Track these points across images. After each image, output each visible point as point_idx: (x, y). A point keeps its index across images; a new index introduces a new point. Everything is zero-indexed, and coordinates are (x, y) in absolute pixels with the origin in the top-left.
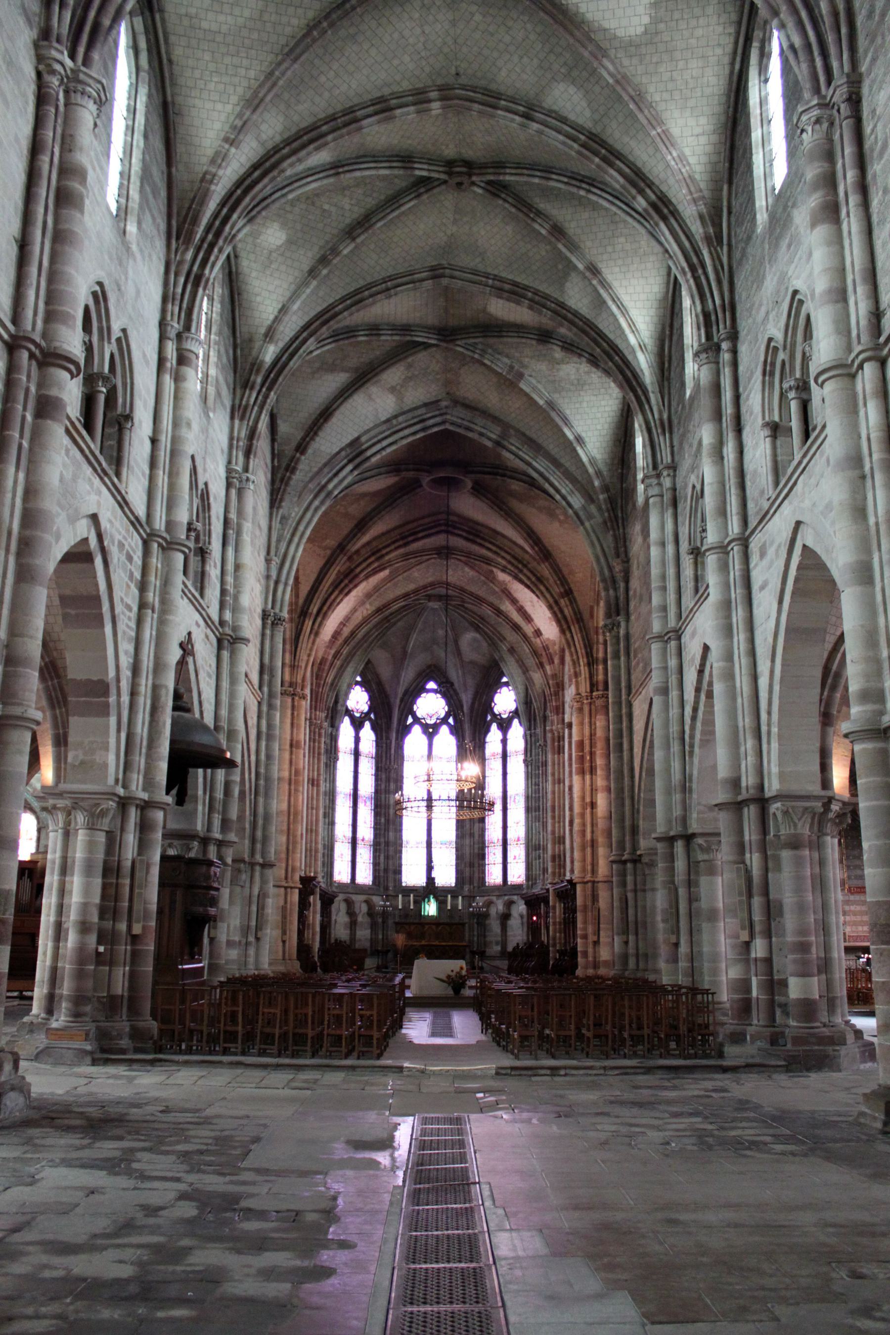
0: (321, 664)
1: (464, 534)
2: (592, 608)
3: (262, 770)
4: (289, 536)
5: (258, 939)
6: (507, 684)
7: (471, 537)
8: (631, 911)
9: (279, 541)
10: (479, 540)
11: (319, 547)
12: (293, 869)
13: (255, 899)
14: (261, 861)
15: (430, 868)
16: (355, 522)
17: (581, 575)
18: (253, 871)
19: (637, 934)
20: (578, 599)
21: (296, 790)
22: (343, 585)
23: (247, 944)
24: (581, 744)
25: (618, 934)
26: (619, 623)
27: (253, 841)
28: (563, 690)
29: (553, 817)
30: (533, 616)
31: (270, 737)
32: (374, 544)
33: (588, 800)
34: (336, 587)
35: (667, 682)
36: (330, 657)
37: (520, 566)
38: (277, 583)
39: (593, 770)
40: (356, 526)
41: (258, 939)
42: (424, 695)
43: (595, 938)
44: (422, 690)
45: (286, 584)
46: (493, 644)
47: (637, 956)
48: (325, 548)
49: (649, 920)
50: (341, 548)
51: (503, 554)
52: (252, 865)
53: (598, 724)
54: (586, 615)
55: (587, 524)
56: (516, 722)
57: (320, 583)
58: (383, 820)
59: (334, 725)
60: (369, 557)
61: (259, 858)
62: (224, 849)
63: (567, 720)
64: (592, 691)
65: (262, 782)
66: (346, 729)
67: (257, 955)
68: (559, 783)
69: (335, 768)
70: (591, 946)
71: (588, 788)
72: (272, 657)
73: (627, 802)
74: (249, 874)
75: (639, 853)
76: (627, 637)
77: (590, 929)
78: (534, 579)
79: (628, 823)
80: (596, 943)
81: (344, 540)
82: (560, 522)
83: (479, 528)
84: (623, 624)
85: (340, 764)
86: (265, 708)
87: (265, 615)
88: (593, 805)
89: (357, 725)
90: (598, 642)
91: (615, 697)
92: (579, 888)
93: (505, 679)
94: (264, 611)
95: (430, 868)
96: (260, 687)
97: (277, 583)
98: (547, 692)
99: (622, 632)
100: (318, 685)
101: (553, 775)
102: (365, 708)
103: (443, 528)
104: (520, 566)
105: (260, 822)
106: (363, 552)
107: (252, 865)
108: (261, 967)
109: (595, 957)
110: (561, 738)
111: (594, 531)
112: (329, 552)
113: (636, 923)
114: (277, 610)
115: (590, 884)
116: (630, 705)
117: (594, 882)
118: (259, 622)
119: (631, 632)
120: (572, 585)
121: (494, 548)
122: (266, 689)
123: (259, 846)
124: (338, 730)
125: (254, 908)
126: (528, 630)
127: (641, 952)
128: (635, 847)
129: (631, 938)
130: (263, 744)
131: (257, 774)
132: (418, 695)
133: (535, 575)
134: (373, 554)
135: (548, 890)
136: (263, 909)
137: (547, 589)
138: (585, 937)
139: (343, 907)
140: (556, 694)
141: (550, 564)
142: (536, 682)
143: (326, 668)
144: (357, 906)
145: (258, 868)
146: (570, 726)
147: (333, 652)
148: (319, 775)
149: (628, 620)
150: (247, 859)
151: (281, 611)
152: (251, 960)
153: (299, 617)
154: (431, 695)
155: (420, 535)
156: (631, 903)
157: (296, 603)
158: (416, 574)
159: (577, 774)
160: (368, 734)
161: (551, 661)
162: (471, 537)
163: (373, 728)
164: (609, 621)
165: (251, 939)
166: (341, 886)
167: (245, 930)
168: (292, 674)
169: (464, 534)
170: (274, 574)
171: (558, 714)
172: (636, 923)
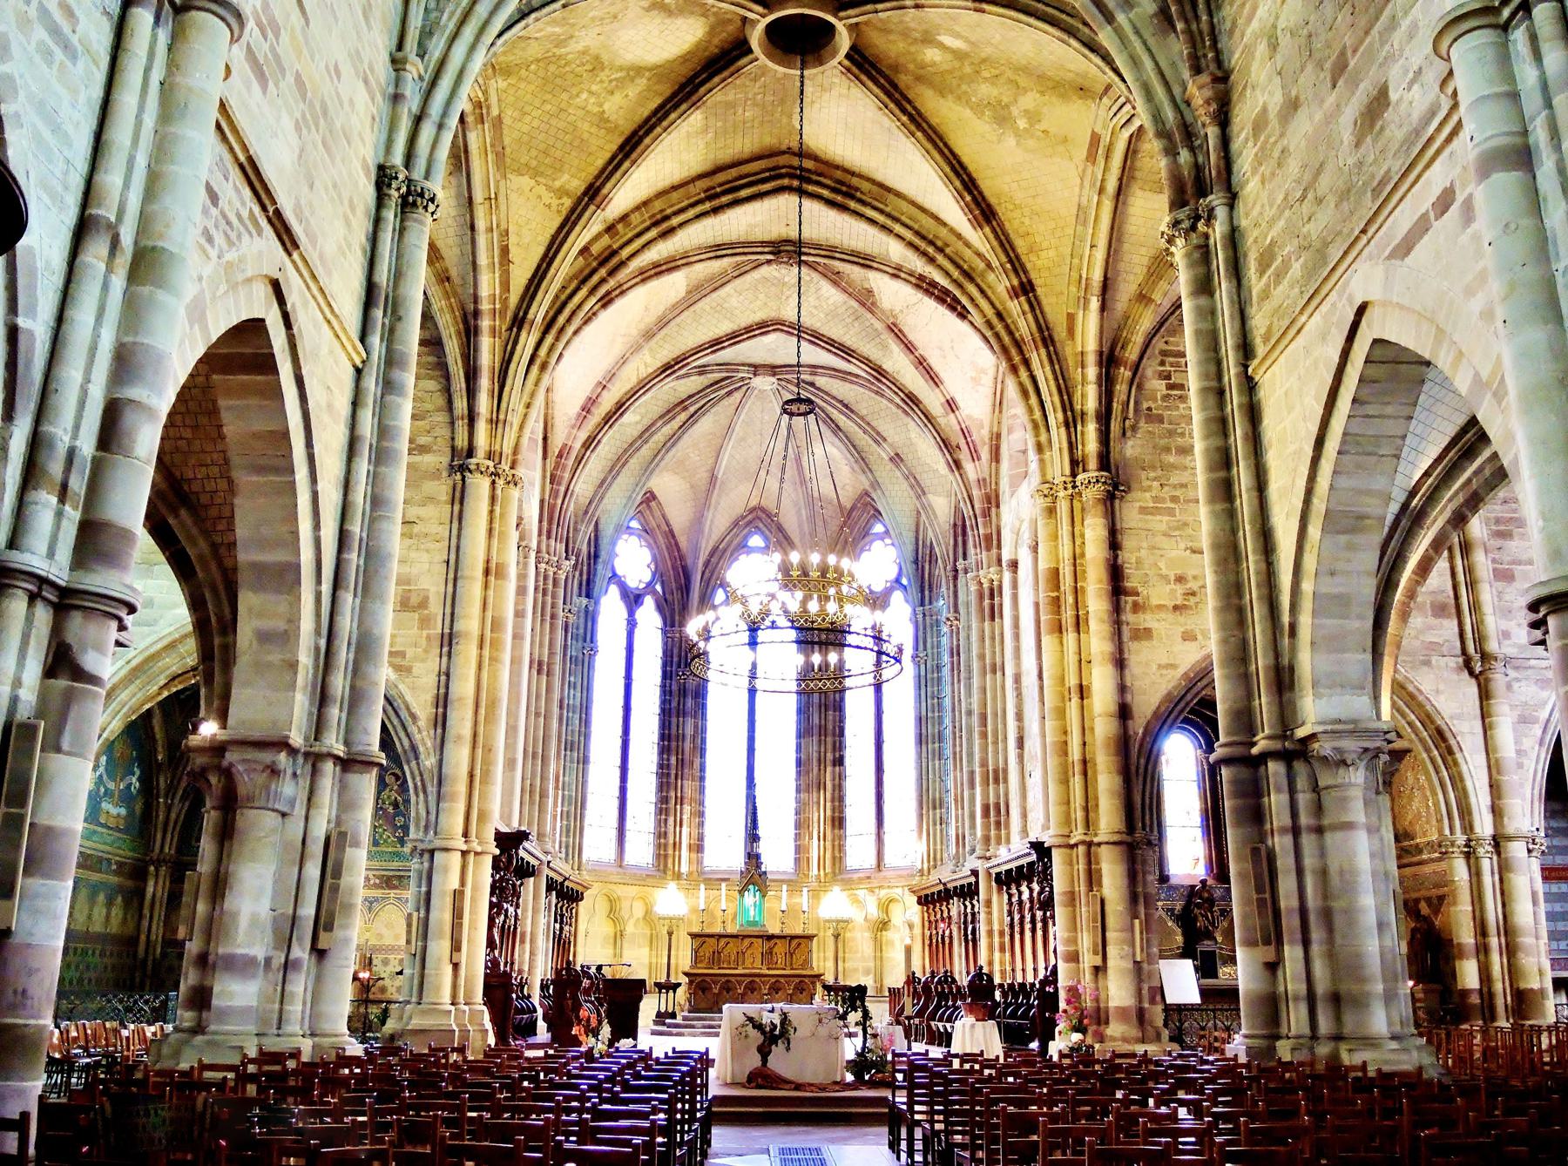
0: (560, 456)
1: (825, 193)
2: (1071, 318)
3: (356, 528)
4: (451, 26)
5: (320, 953)
6: (881, 537)
7: (839, 198)
8: (1287, 885)
9: (427, 33)
10: (853, 204)
11: (549, 188)
12: (483, 817)
13: (316, 849)
14: (340, 750)
15: (753, 837)
16: (620, 140)
17: (1052, 253)
18: (315, 772)
19: (1306, 943)
20: (1045, 301)
21: (494, 660)
22: (595, 279)
23: (288, 966)
24: (1055, 574)
25: (1250, 943)
26: (1211, 211)
27: (322, 698)
28: (998, 506)
29: (984, 735)
30: (942, 375)
31: (381, 456)
32: (658, 205)
33: (1072, 681)
34: (584, 282)
35: (1525, 133)
36: (578, 445)
37: (931, 250)
38: (418, 120)
39: (1079, 624)
40: (621, 148)
41: (320, 953)
42: (743, 558)
43: (1098, 961)
44: (743, 547)
45: (440, 126)
46: (862, 460)
47: (1311, 998)
48: (561, 192)
49: (1337, 905)
50: (593, 194)
51: (898, 228)
52: (315, 759)
53: (1089, 534)
54: (1060, 332)
55: (1121, 18)
56: (897, 597)
57: (549, 265)
58: (673, 760)
59: (588, 589)
60: (648, 229)
61: (334, 743)
62: (77, 627)
63: (1006, 556)
64: (1074, 475)
65: (353, 558)
66: (611, 607)
67: (316, 997)
68: (994, 672)
69: (591, 667)
70: (1088, 977)
71: (1071, 658)
72: (398, 275)
73: (1258, 613)
74: (305, 783)
75: (1301, 733)
76: (1234, 238)
77: (1086, 942)
78: (956, 274)
79: (1261, 661)
80: (1099, 971)
81: (597, 177)
82: (1018, 134)
83: (855, 181)
84: (1221, 213)
85: (600, 662)
86: (371, 384)
87: (383, 177)
88: (1083, 692)
89: (633, 600)
90: (1084, 381)
91: (1205, 376)
92: (1056, 855)
93: (878, 528)
94: (381, 168)
95: (753, 837)
96: (363, 339)
97: (418, 120)
98: (967, 511)
99: (1218, 230)
100: (554, 493)
101: (982, 657)
102: (647, 576)
103: (786, 182)
104: (931, 250)
105: (343, 655)
106: (635, 218)
107: (315, 759)
108: (326, 1027)
109: (1097, 1000)
110: (994, 592)
111: (1137, 32)
112: (568, 203)
113: (1303, 912)
114: (418, 174)
115: (1081, 849)
116: (1250, 385)
117: (1089, 844)
118: (370, 192)
119: (1244, 223)
120: (1033, 276)
121: (881, 218)
122: (375, 340)
123: (335, 713)
124: (597, 603)
125: (313, 871)
126: (932, 400)
127: (1321, 988)
128: (1286, 717)
129: (1292, 954)
130: (363, 467)
131: (343, 538)
132: (733, 558)
133: (958, 266)
134: (656, 224)
135: (975, 873)
136: (337, 874)
137: (982, 291)
138: (1074, 957)
139: (602, 907)
140: (986, 514)
141: (994, 230)
142: (939, 513)
143: (571, 462)
144: (625, 905)
145: (329, 767)
146: (1014, 565)
147: (583, 436)
148: (551, 654)
149: (1232, 199)
150: (297, 739)
151: (427, 176)
152: (296, 1008)
153: (510, 329)
154: (756, 557)
155: (744, 193)
156: (1285, 862)
157: (505, 301)
158: (734, 302)
159: (1051, 632)
160: (649, 616)
161: (975, 455)
162: (839, 198)
163: (659, 608)
164: (1182, 214)
165: (301, 952)
166: (599, 870)
167: (286, 931)
168: (492, 435)
169: (825, 193)
170: (412, 103)
171: (988, 549)
172: (1303, 912)
